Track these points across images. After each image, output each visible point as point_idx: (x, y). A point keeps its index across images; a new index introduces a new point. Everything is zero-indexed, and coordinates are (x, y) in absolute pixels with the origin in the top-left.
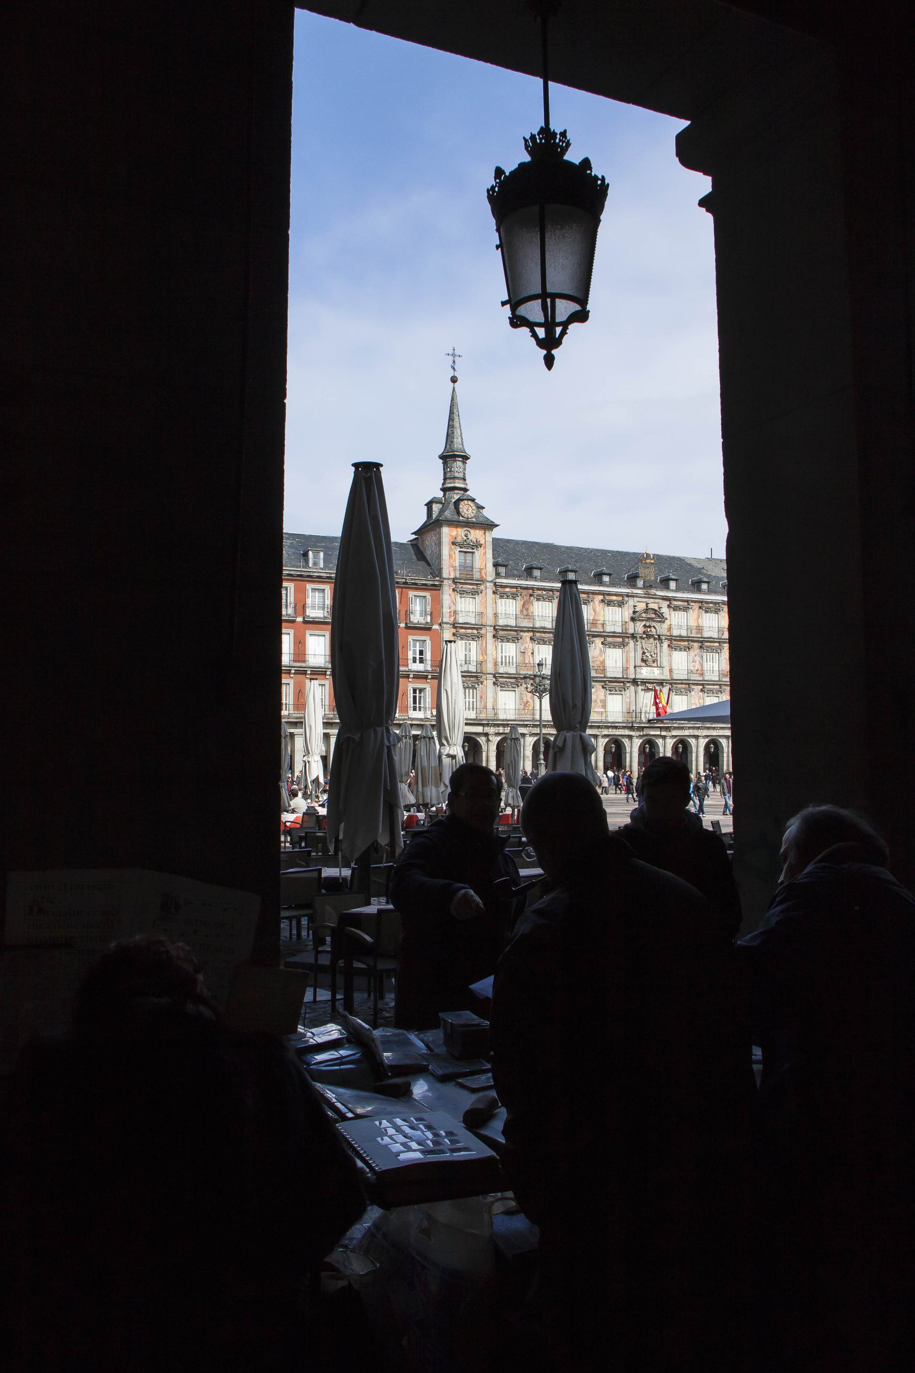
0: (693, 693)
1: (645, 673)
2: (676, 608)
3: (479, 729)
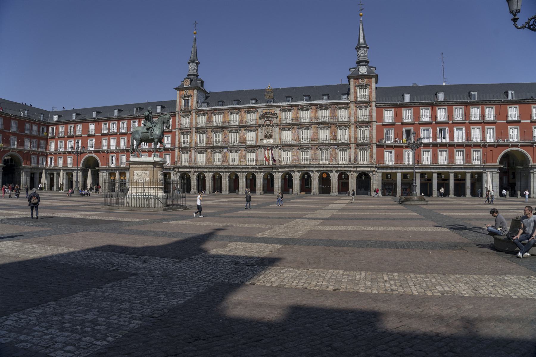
1: (265, 142)
2: (284, 111)
3: (188, 170)
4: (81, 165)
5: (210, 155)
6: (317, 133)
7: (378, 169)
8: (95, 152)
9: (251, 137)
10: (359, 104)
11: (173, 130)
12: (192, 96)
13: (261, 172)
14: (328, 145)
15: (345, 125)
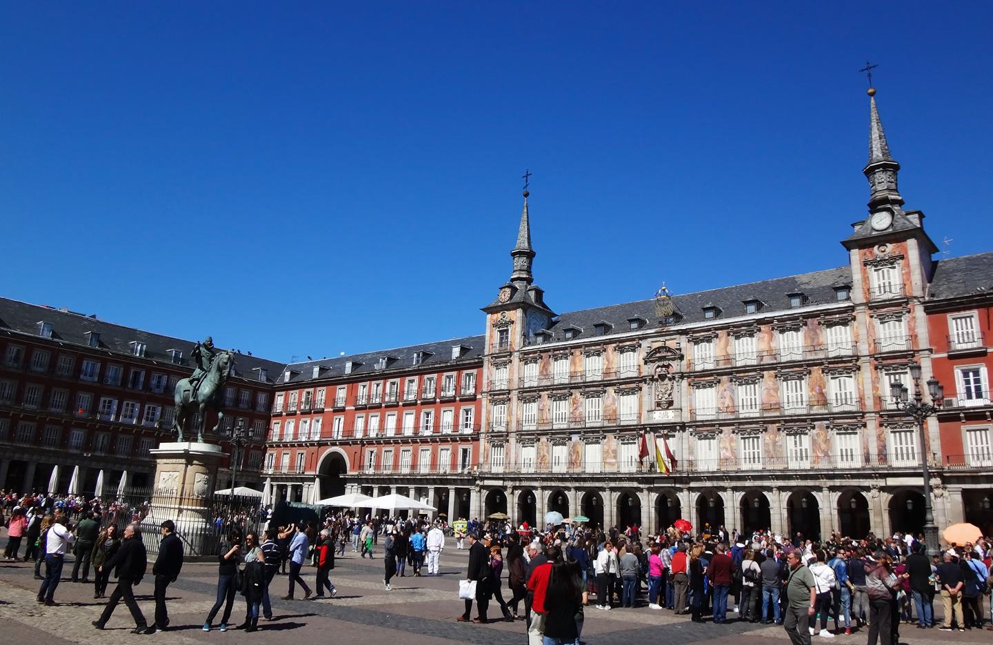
0: (722, 435)
1: (660, 417)
2: (697, 341)
3: (500, 483)
4: (318, 469)
5: (545, 449)
6: (776, 390)
7: (946, 480)
8: (342, 444)
9: (628, 409)
10: (878, 307)
11: (479, 396)
12: (513, 322)
13: (650, 490)
14: (804, 421)
15: (844, 365)
